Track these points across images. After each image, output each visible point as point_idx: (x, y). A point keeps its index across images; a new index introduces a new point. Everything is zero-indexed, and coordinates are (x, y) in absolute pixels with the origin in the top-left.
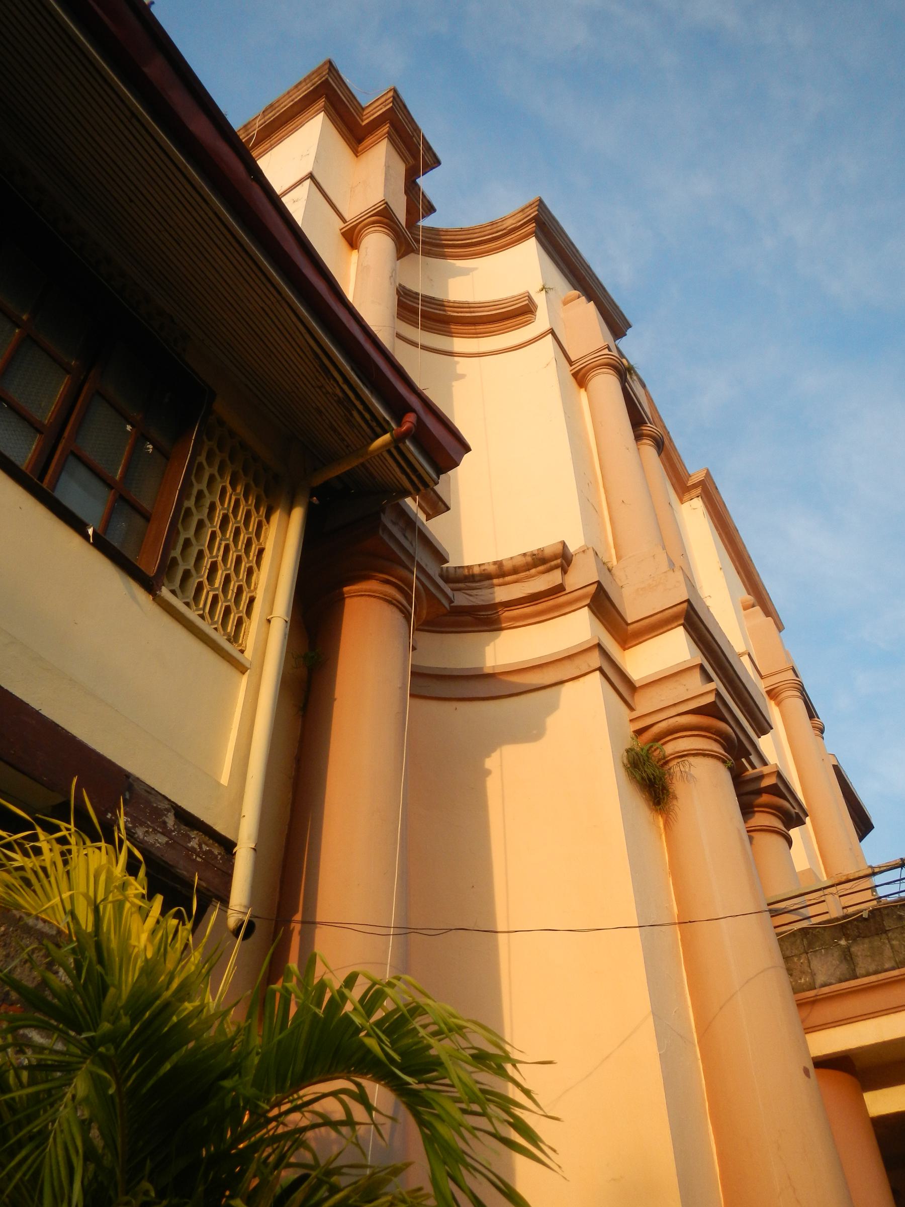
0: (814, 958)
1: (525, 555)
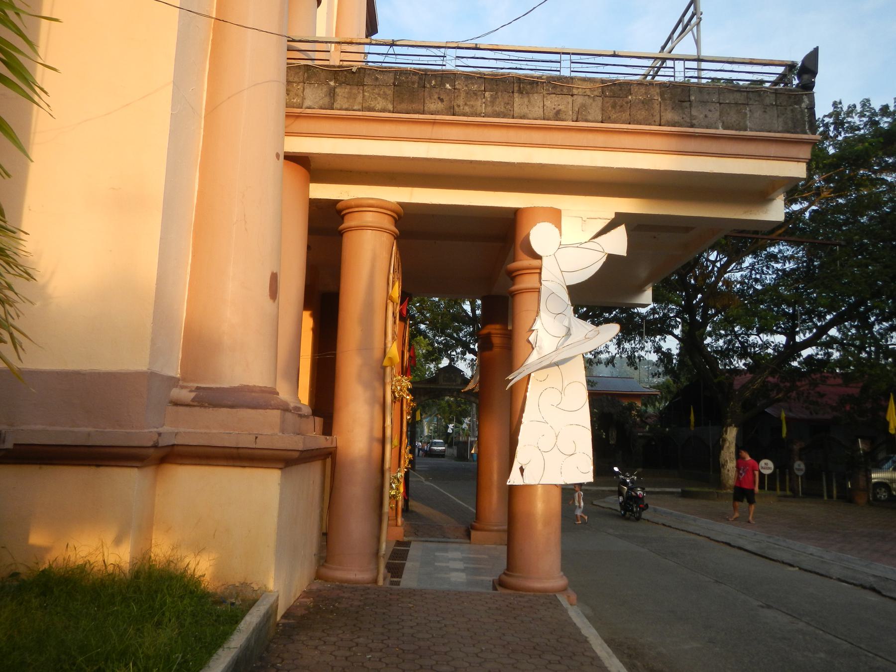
0: (308, 87)
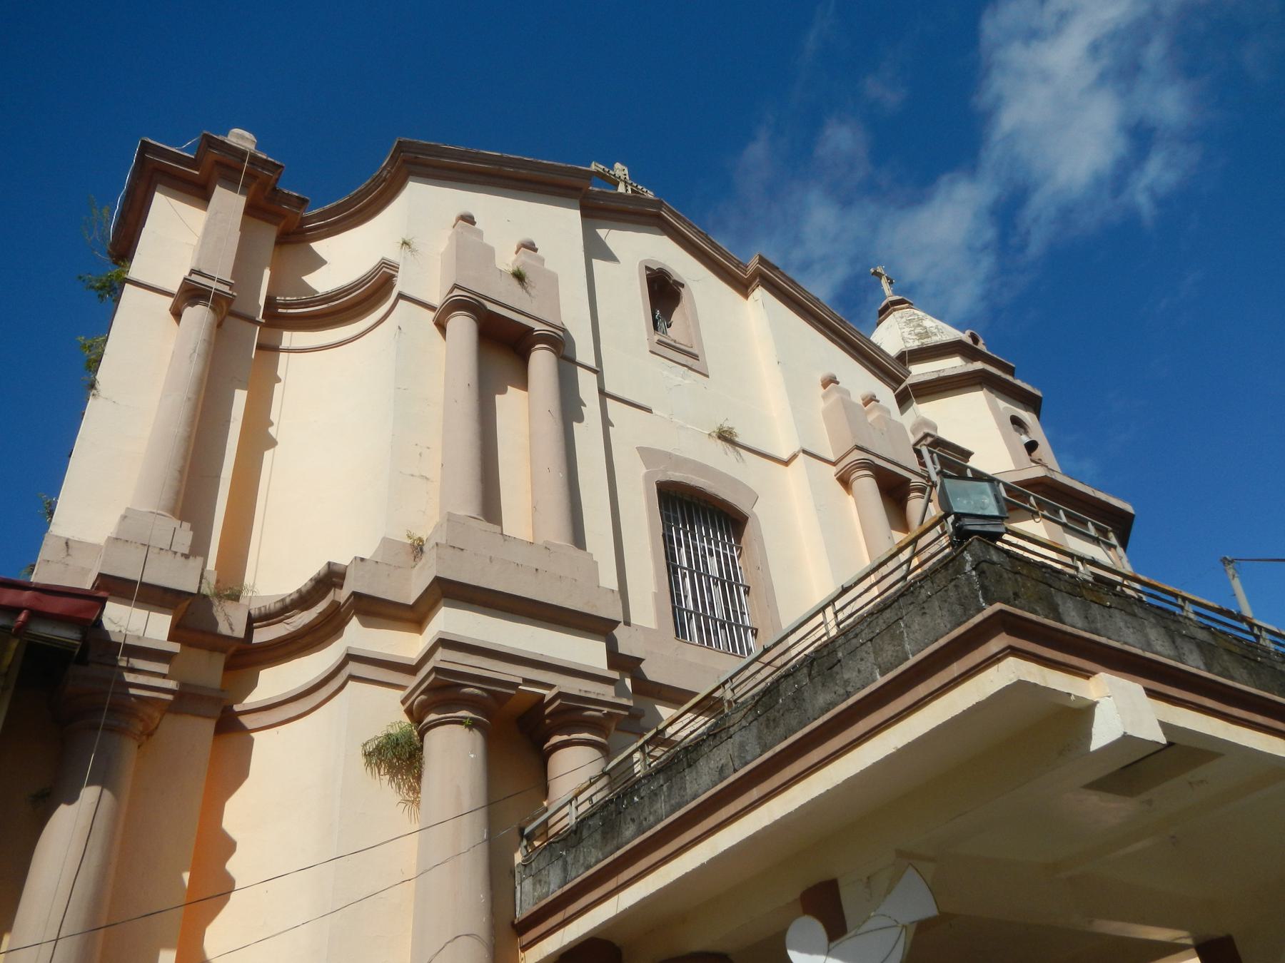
1: (311, 580)
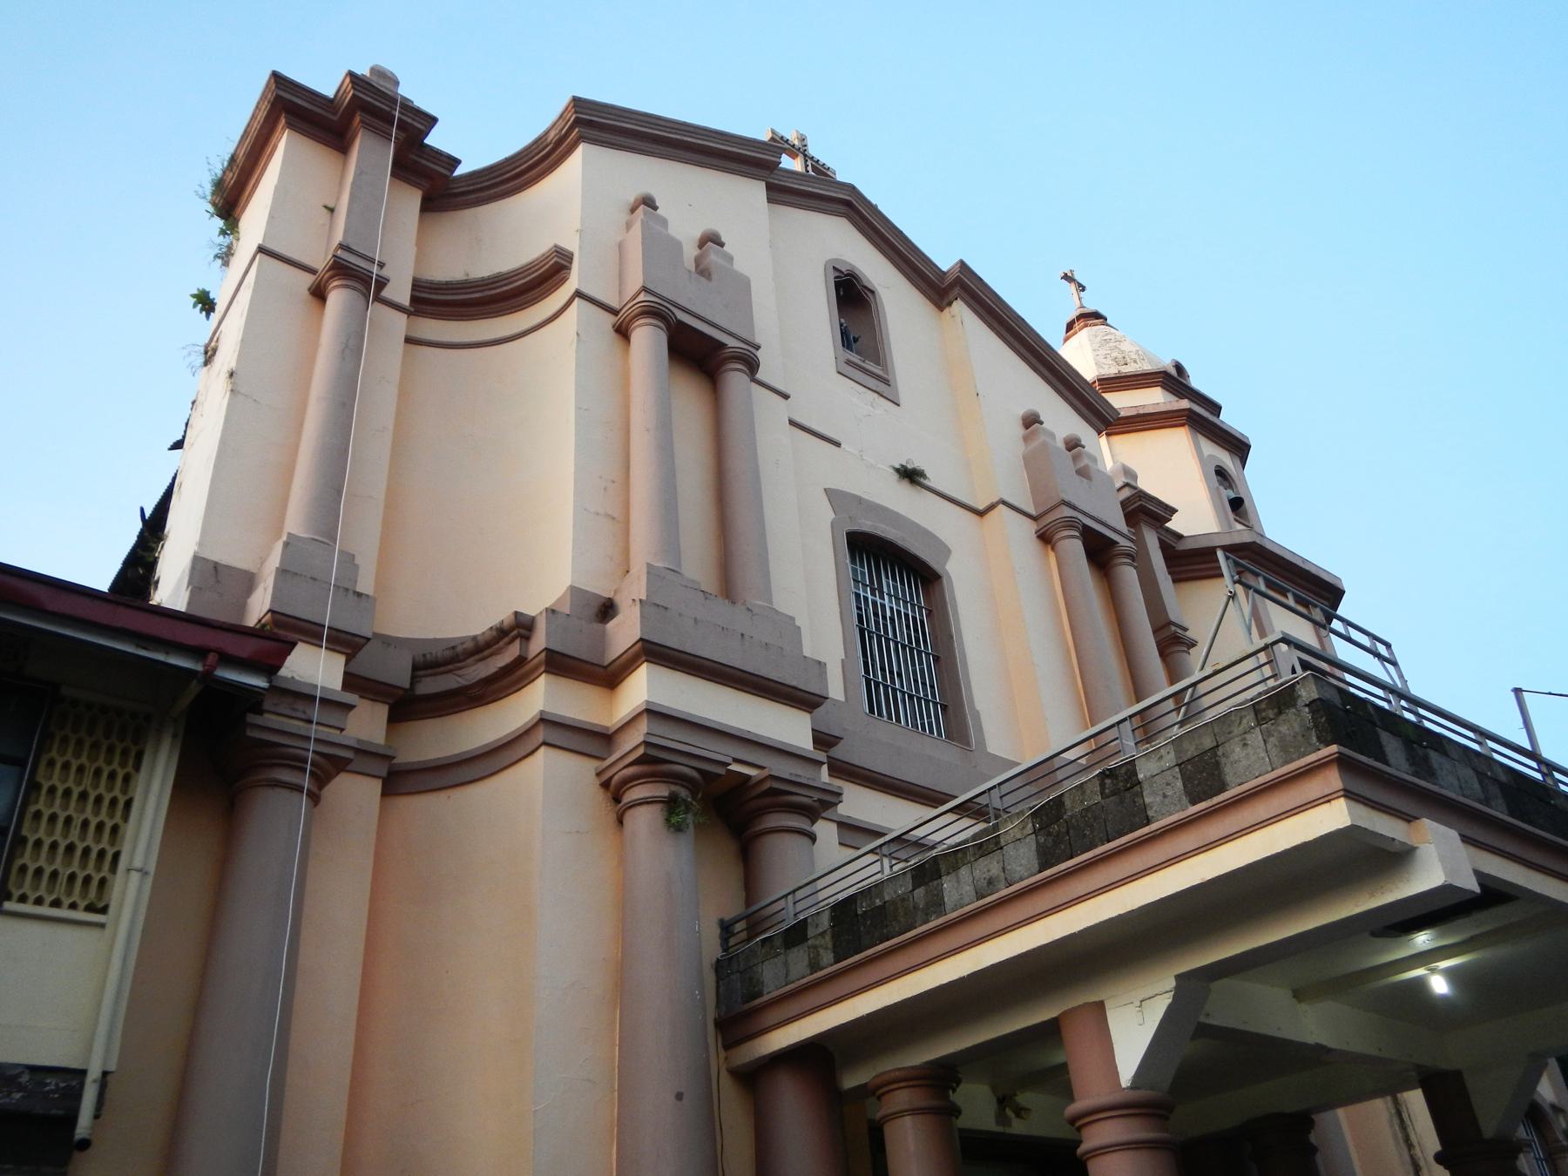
1: (491, 628)
